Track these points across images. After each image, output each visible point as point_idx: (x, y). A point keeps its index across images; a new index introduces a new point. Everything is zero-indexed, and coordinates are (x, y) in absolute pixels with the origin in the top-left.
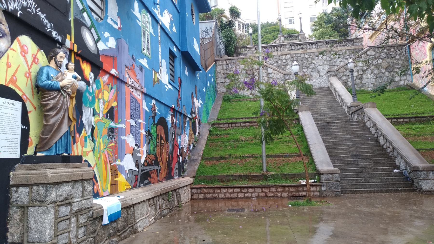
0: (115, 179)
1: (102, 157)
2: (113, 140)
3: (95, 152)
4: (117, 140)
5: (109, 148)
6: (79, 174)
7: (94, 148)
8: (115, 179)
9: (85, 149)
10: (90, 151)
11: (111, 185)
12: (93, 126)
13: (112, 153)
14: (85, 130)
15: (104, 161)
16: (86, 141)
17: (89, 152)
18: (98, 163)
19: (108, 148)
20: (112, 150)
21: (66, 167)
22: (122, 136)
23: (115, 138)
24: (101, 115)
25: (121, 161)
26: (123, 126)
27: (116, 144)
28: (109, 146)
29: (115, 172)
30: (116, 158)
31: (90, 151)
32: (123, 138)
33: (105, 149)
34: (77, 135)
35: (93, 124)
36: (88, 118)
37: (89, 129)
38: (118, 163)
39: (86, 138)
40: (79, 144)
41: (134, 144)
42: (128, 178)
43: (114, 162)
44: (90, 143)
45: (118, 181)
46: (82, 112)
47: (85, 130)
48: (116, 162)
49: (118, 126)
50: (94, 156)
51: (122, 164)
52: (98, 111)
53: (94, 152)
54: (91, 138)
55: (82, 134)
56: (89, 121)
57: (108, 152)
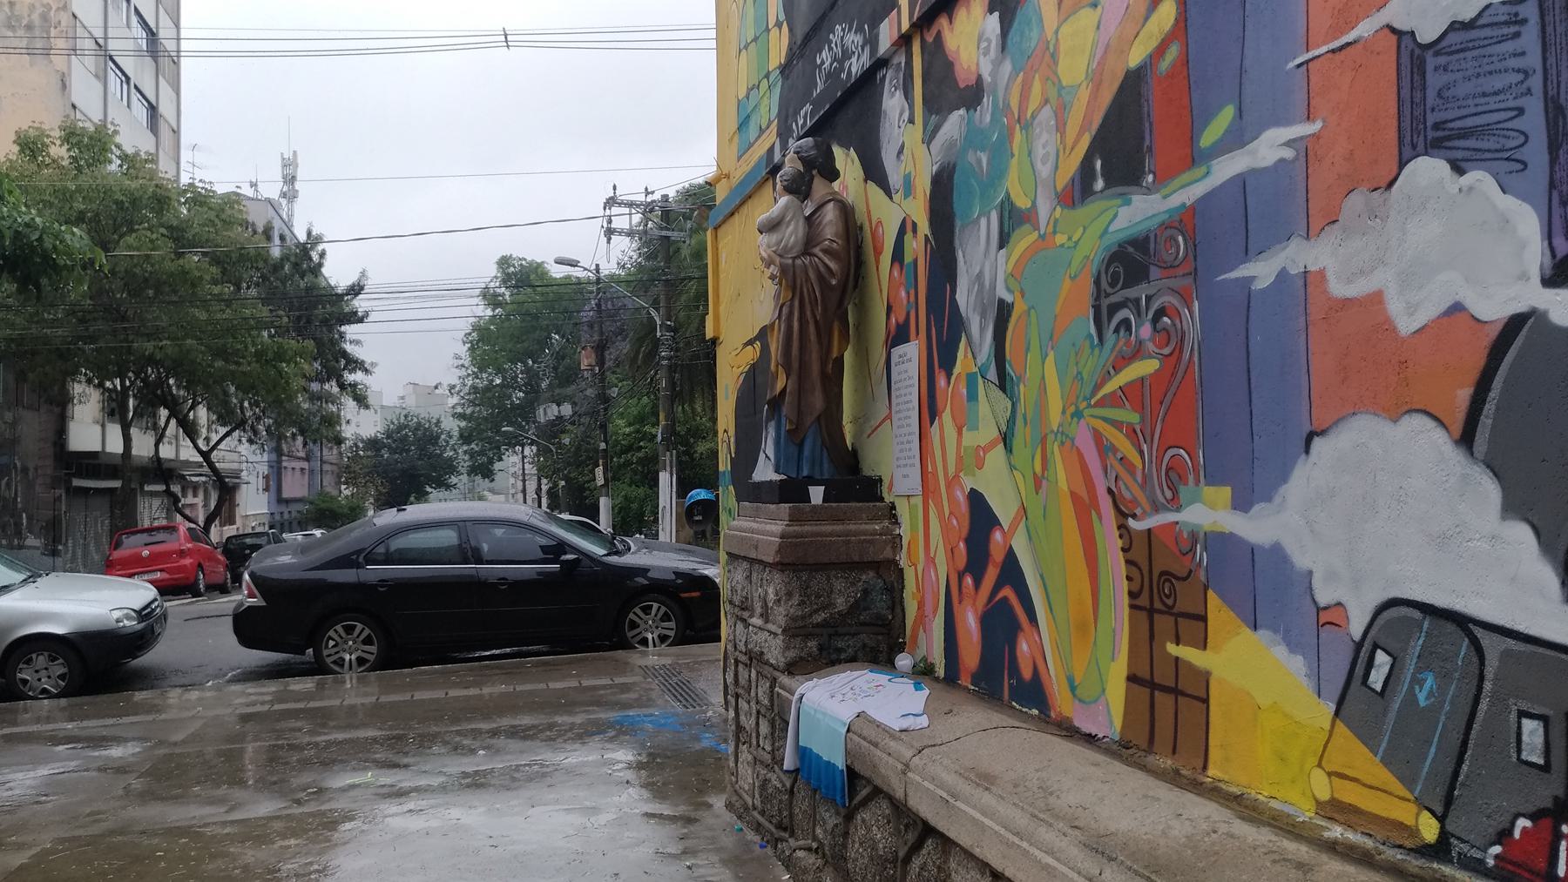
0: (1172, 649)
1: (1061, 476)
2: (1146, 331)
3: (1017, 443)
4: (1192, 320)
5: (1113, 400)
6: (751, 539)
7: (1011, 421)
8: (1172, 649)
9: (970, 439)
10: (992, 445)
11: (1132, 678)
12: (1001, 302)
13: (1132, 433)
14: (969, 343)
15: (1073, 494)
16: (972, 396)
17: (986, 449)
18: (1035, 512)
19: (1101, 403)
20: (1134, 418)
21: (755, 516)
22: (1246, 254)
23: (1161, 312)
24: (1045, 208)
25: (1241, 504)
26: (1270, 148)
27: (1172, 361)
28: (1111, 387)
29: (1168, 592)
30: (1174, 477)
31: (992, 445)
32: (1261, 271)
33: (1078, 414)
34: (941, 381)
35: (1002, 292)
36: (980, 276)
37: (982, 330)
38: (1207, 511)
39: (971, 381)
40: (947, 416)
41: (1535, 255)
42: (1352, 699)
43: (1157, 508)
44: (990, 408)
45: (1205, 677)
46: (954, 261)
47: (969, 343)
48: (1175, 503)
49: (1188, 192)
50: (1012, 467)
51: (1254, 528)
52: (1022, 202)
53: (1009, 449)
54: (992, 374)
55: (957, 370)
56: (981, 285)
57: (1098, 437)
